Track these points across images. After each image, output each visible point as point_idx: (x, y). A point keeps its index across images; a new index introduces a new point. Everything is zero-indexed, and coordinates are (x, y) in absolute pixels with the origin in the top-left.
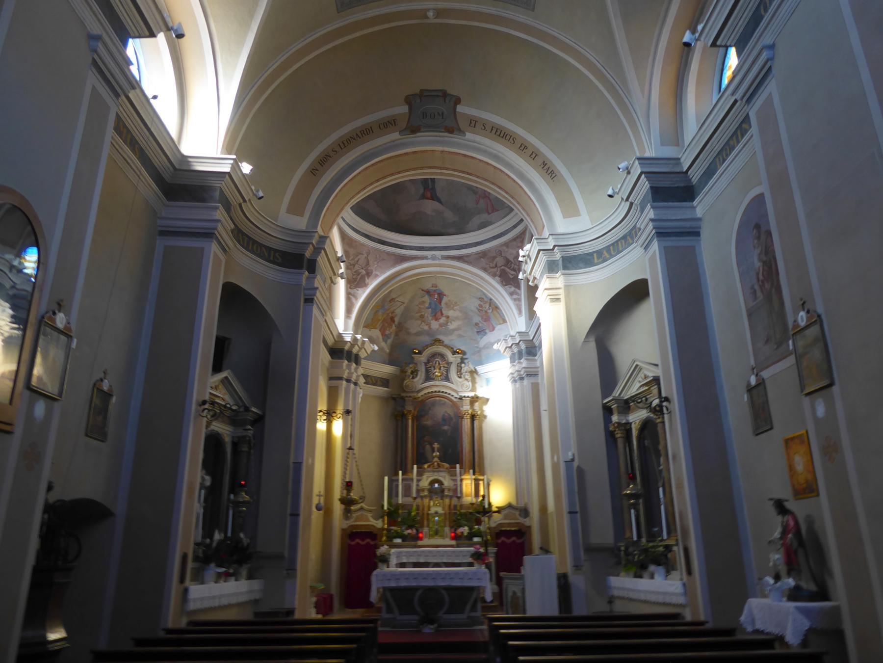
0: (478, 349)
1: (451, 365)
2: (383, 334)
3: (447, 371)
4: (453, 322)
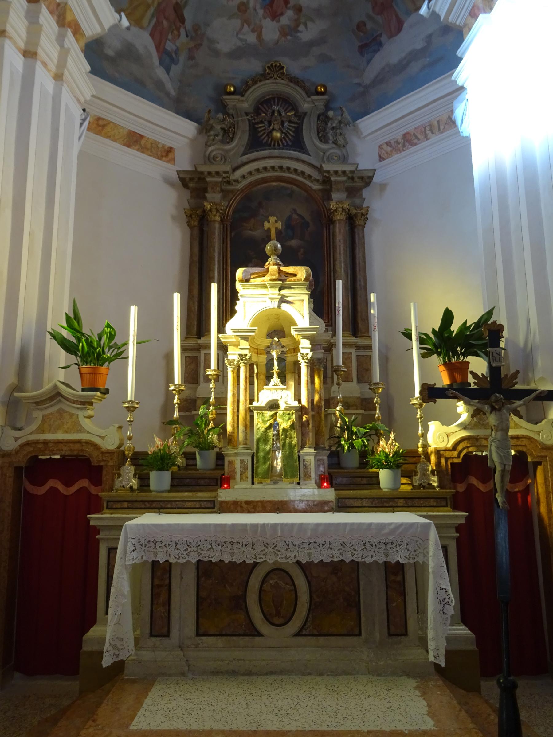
0: (361, 89)
1: (304, 119)
2: (159, 46)
3: (298, 131)
4: (309, 24)
